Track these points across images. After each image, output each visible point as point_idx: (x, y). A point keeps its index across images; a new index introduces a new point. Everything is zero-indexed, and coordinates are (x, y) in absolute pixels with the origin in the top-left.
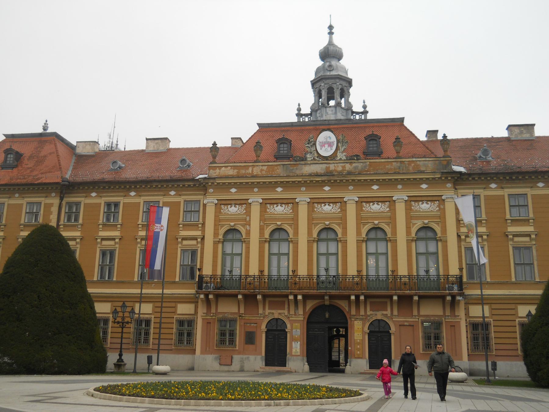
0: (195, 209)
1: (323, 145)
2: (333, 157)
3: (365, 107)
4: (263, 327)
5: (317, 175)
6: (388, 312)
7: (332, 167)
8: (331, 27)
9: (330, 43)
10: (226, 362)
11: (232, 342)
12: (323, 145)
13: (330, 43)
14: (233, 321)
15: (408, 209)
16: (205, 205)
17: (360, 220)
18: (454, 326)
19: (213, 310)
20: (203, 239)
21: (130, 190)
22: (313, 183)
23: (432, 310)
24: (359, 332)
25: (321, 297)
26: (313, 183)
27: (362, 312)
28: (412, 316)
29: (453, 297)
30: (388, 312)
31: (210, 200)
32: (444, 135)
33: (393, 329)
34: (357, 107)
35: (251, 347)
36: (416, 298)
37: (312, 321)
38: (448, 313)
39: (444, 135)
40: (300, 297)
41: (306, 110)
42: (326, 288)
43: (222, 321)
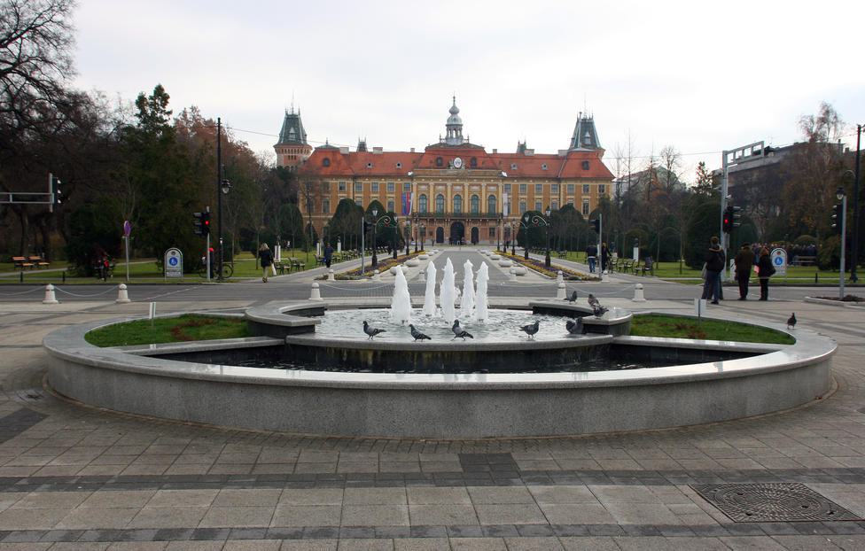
0: (408, 188)
2: (460, 168)
9: (454, 107)
11: (425, 235)
13: (454, 107)
23: (492, 224)
24: (468, 231)
31: (415, 183)
34: (465, 138)
37: (453, 227)
41: (444, 136)
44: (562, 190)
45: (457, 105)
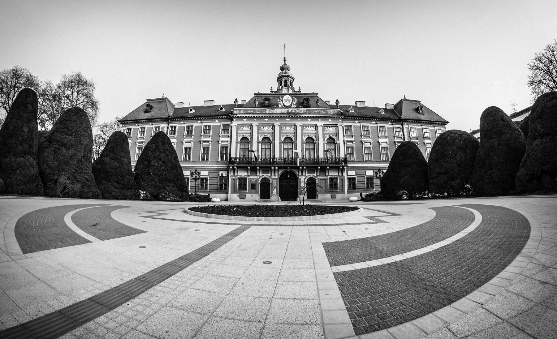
0: (227, 129)
1: (286, 101)
2: (290, 106)
3: (299, 89)
4: (259, 181)
5: (283, 113)
6: (315, 174)
7: (290, 111)
8: (285, 58)
9: (285, 64)
10: (243, 197)
11: (245, 188)
12: (286, 101)
13: (285, 64)
14: (245, 179)
15: (323, 130)
16: (232, 127)
17: (303, 134)
18: (342, 180)
19: (236, 174)
20: (231, 142)
21: (198, 120)
22: (281, 117)
24: (303, 182)
25: (286, 168)
26: (281, 117)
27: (304, 174)
28: (326, 176)
29: (343, 167)
30: (315, 174)
31: (235, 124)
32: (337, 100)
33: (317, 182)
35: (254, 191)
36: (328, 168)
37: (282, 179)
38: (340, 174)
39: (337, 100)
40: (277, 168)
42: (289, 164)
43: (240, 179)
44: (406, 134)
45: (286, 63)
